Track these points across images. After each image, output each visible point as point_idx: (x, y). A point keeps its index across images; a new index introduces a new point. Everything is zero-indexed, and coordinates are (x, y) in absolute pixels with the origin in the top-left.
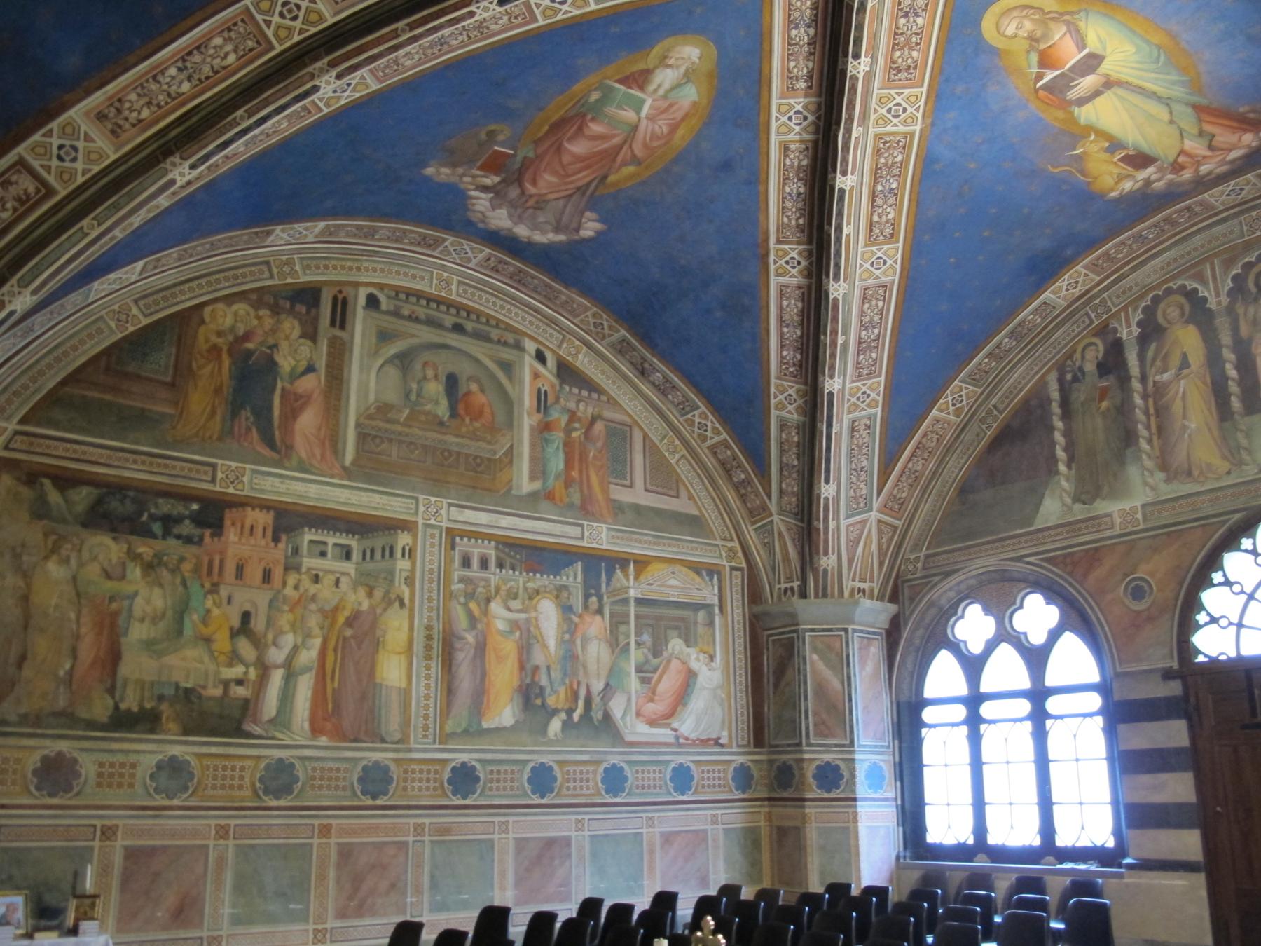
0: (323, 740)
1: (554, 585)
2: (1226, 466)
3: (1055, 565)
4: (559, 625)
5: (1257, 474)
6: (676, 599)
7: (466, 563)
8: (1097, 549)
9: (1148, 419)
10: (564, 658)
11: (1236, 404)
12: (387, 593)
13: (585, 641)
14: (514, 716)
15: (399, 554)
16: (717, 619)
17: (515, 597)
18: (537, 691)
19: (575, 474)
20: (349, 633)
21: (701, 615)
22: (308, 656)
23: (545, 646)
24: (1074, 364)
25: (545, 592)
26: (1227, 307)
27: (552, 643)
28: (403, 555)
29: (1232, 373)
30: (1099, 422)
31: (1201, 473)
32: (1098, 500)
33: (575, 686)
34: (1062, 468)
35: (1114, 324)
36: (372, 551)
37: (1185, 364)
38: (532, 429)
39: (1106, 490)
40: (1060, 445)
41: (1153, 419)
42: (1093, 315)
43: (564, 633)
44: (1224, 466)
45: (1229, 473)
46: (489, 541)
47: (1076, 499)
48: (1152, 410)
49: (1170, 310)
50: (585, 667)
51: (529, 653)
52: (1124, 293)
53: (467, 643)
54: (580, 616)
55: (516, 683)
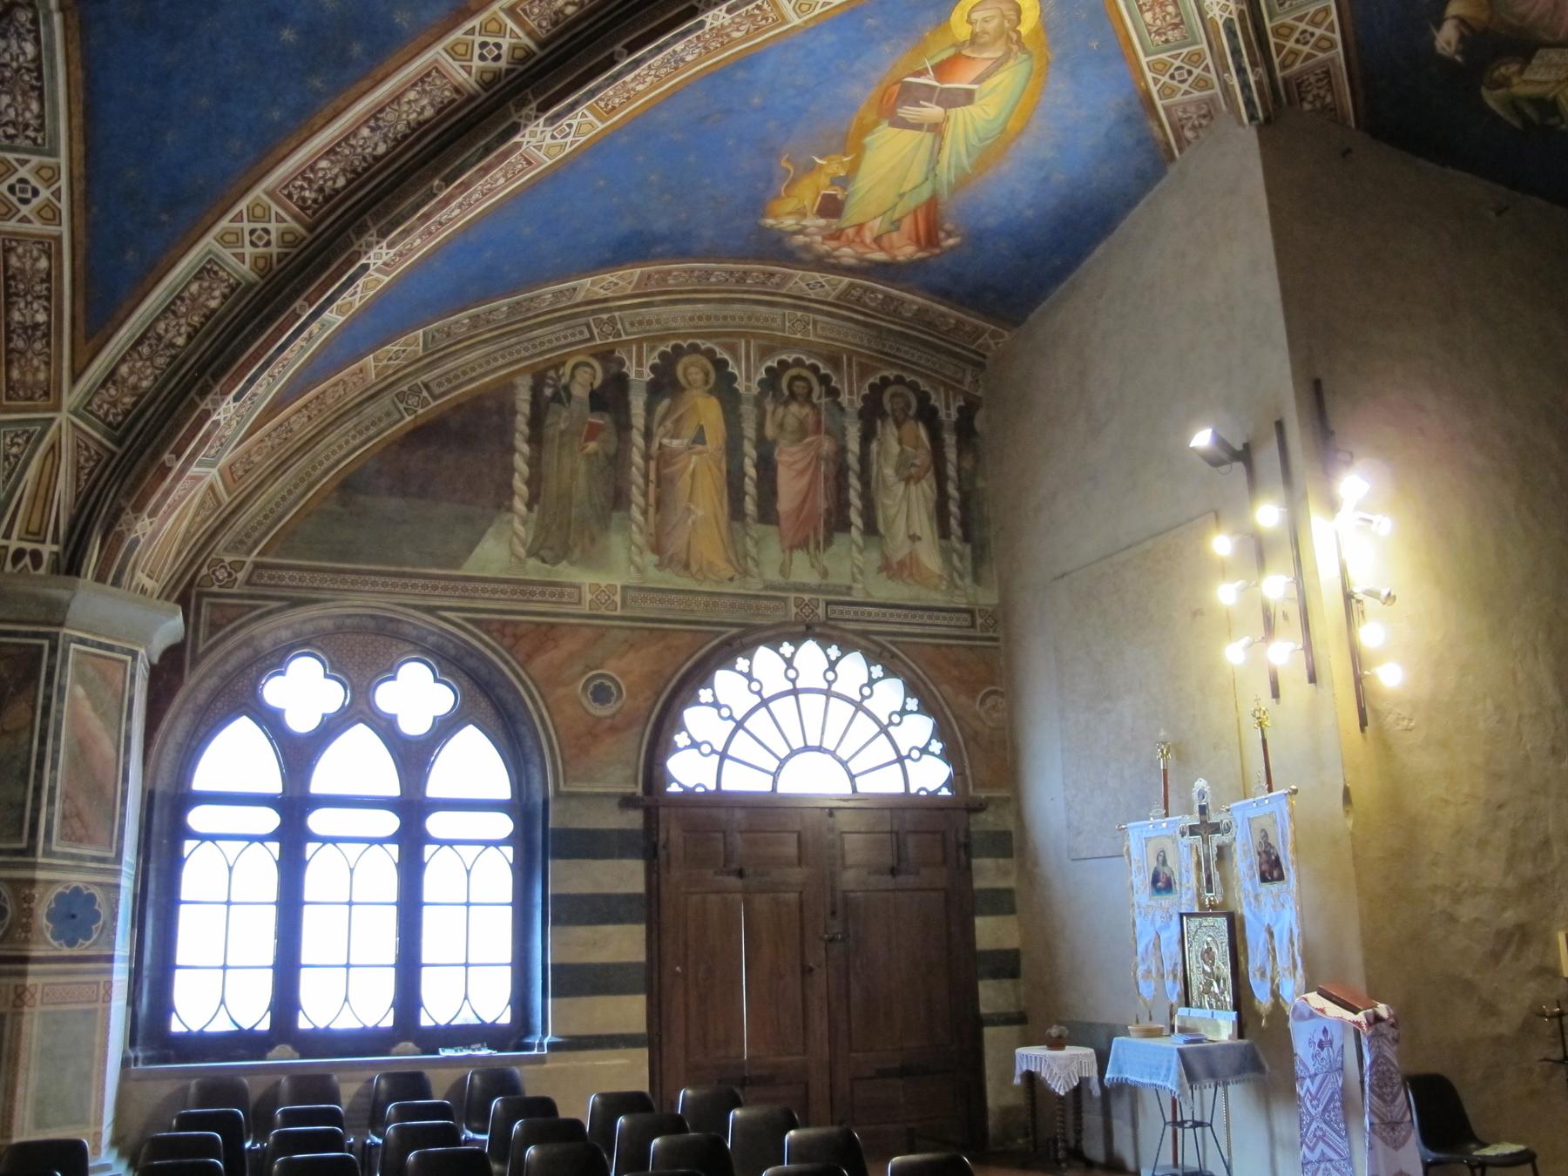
2: (730, 572)
3: (488, 632)
5: (759, 590)
8: (552, 626)
9: (647, 485)
11: (750, 506)
24: (559, 378)
26: (755, 397)
29: (751, 471)
30: (582, 467)
31: (700, 569)
32: (564, 563)
34: (519, 505)
35: (620, 353)
37: (700, 438)
39: (577, 553)
40: (520, 473)
41: (652, 487)
42: (595, 331)
44: (725, 570)
45: (731, 579)
47: (532, 553)
48: (652, 476)
49: (692, 370)
52: (640, 323)
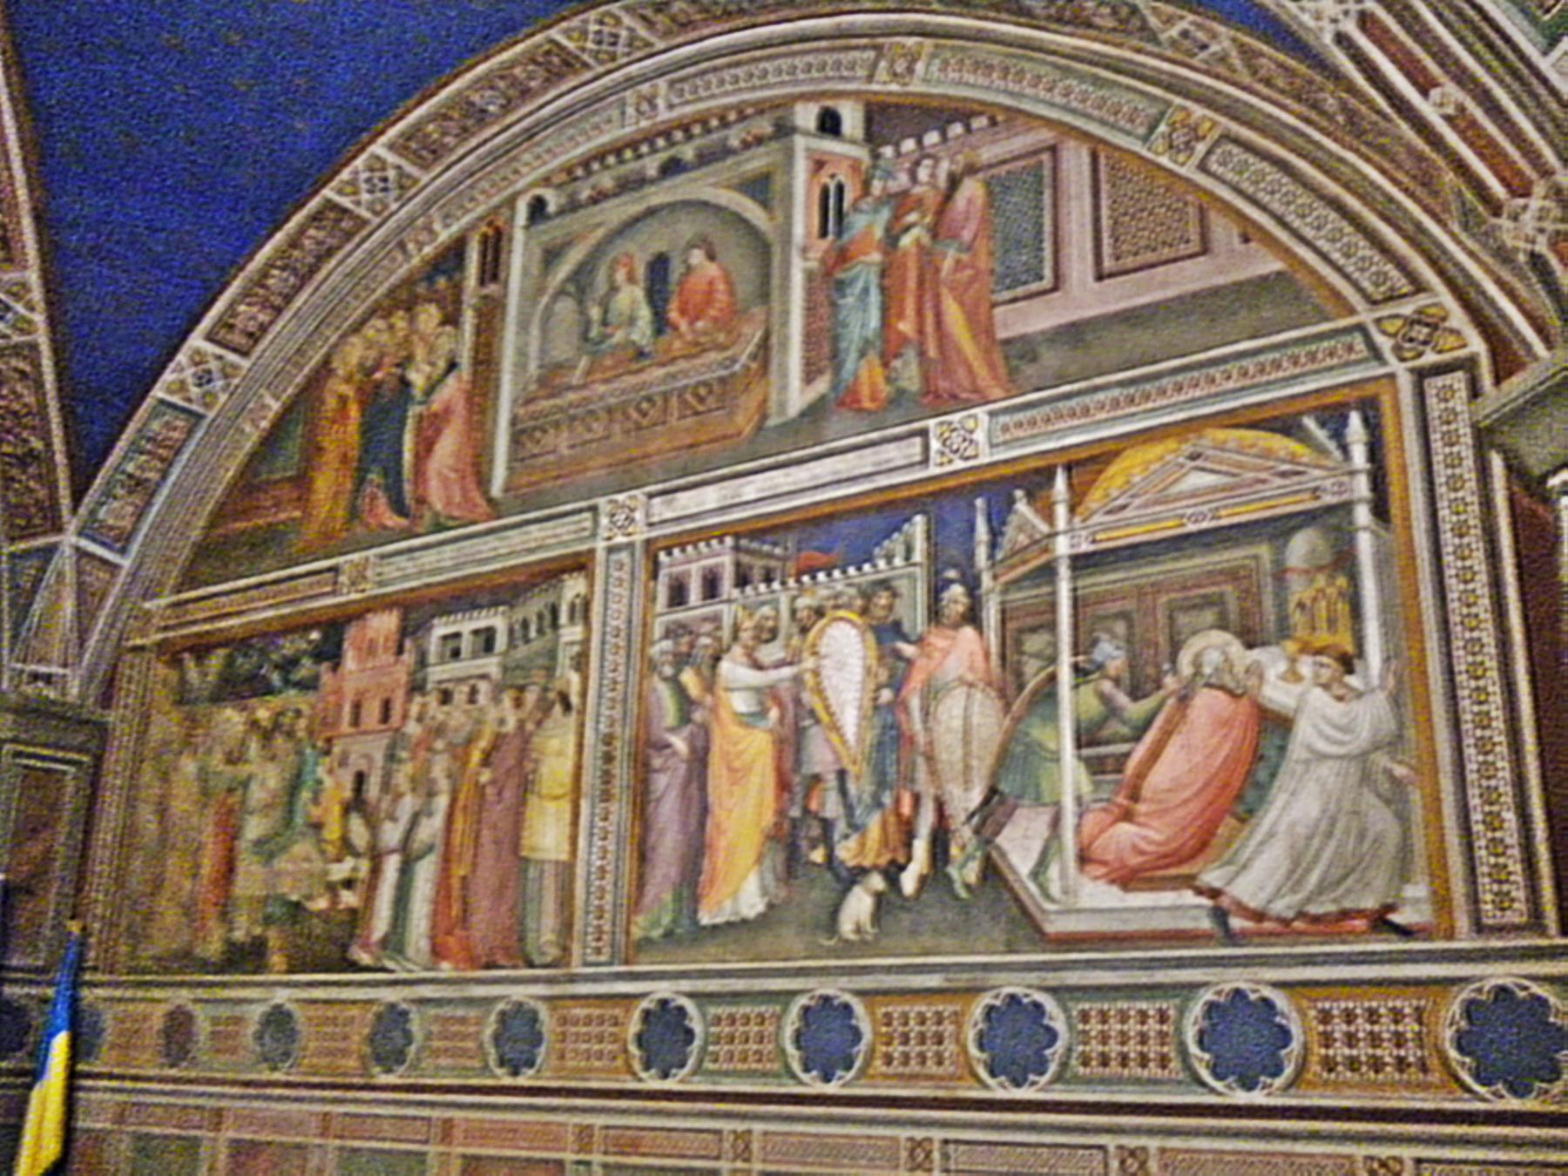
0: (446, 969)
1: (858, 586)
4: (868, 671)
6: (1205, 525)
7: (678, 595)
10: (880, 746)
12: (545, 689)
13: (932, 694)
14: (764, 891)
15: (563, 618)
16: (1365, 545)
17: (774, 634)
18: (816, 831)
19: (906, 327)
20: (485, 776)
21: (1301, 546)
22: (431, 828)
23: (836, 728)
25: (837, 607)
27: (850, 720)
28: (572, 618)
33: (906, 809)
36: (525, 625)
38: (810, 276)
43: (879, 688)
46: (721, 539)
50: (930, 758)
51: (798, 749)
53: (675, 754)
54: (919, 641)
55: (769, 818)
